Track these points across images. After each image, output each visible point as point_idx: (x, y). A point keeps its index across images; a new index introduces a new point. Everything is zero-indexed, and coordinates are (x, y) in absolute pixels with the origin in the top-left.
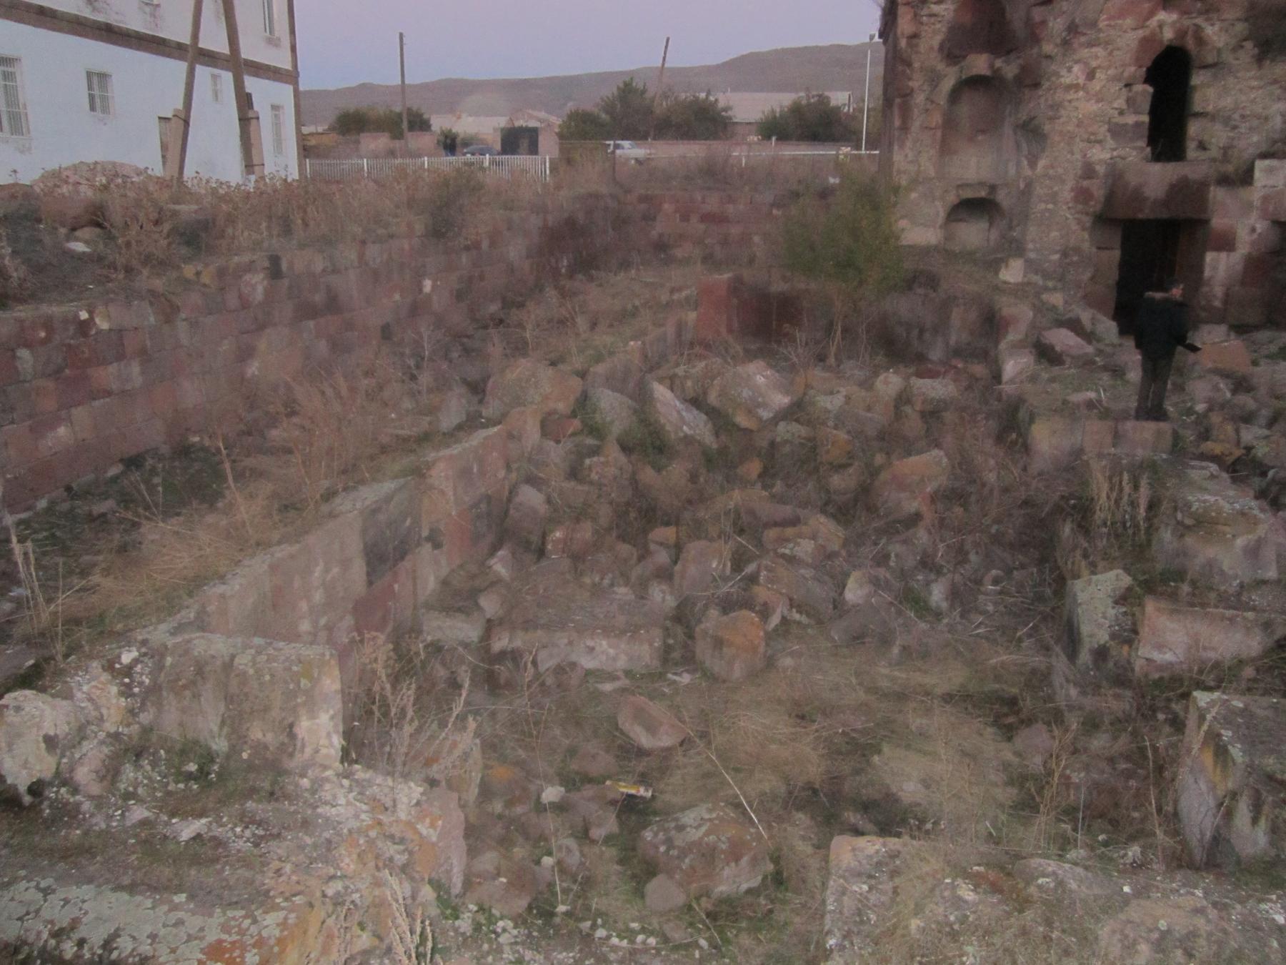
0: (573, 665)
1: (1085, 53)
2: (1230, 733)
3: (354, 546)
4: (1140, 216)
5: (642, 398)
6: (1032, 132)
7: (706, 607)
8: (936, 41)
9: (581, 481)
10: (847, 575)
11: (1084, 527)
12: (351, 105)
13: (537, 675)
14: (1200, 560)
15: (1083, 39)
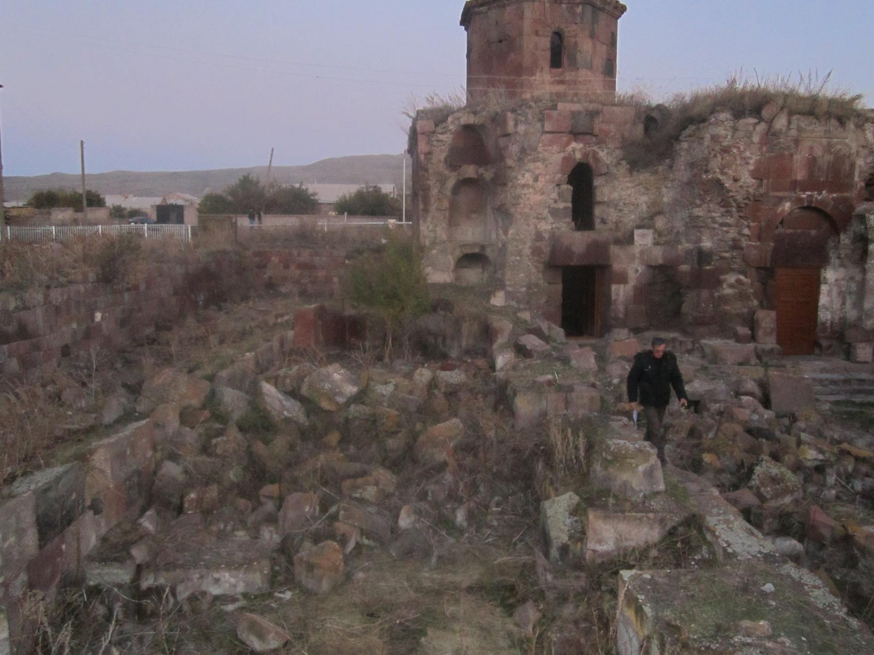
0: (204, 593)
1: (531, 166)
2: (643, 597)
3: (28, 518)
4: (572, 264)
5: (255, 392)
6: (504, 213)
7: (302, 540)
8: (443, 156)
9: (210, 455)
10: (399, 509)
11: (550, 464)
12: (45, 187)
13: (176, 603)
14: (618, 483)
15: (530, 157)
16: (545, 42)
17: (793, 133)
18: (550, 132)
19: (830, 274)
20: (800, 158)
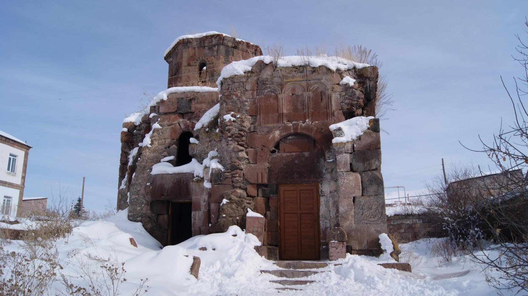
17: (276, 80)
18: (166, 114)
19: (326, 188)
20: (284, 96)
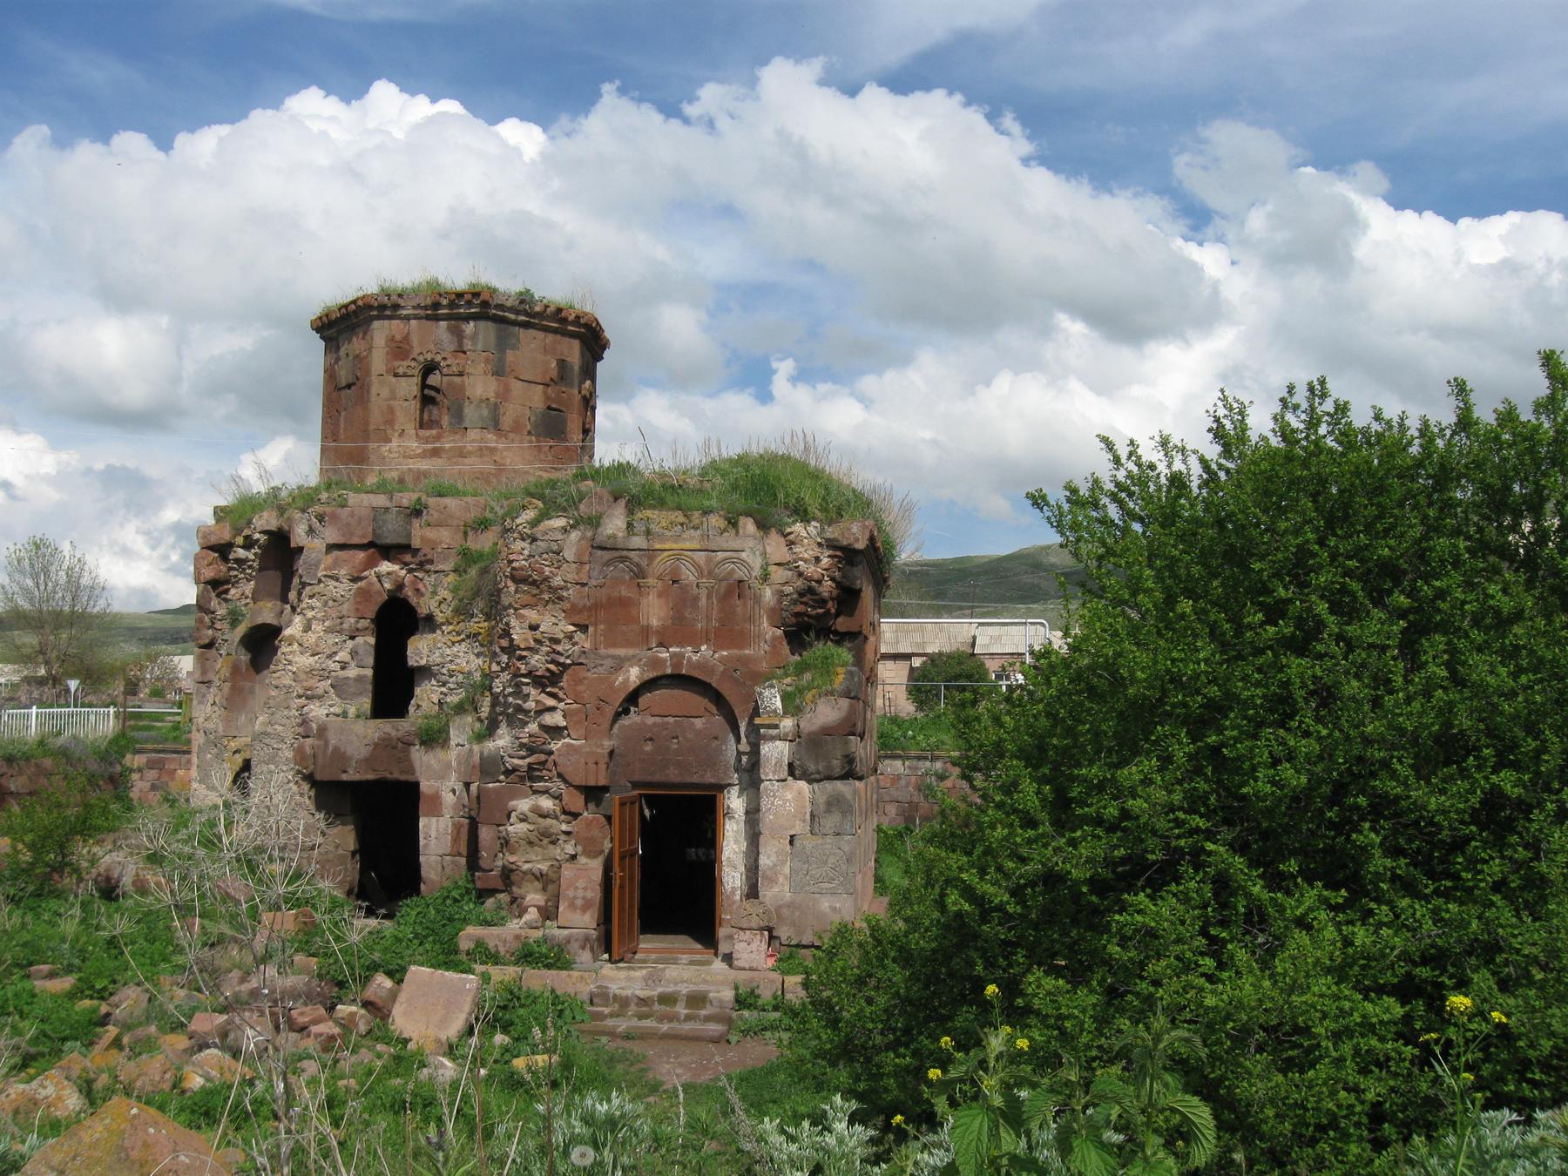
4: (344, 777)
16: (411, 387)
